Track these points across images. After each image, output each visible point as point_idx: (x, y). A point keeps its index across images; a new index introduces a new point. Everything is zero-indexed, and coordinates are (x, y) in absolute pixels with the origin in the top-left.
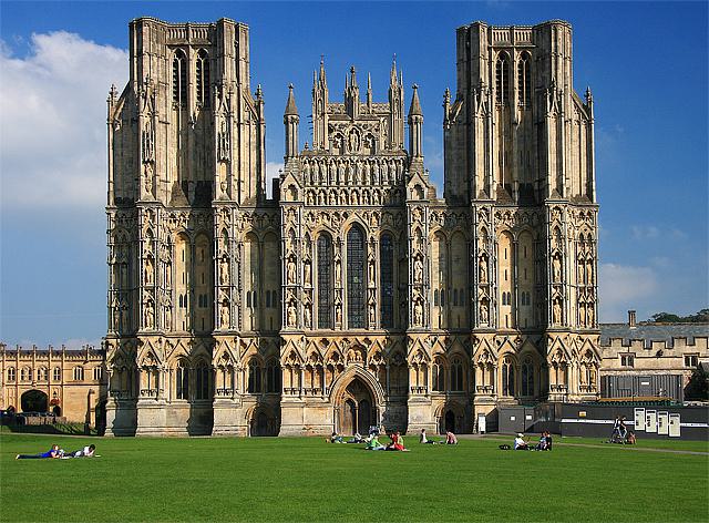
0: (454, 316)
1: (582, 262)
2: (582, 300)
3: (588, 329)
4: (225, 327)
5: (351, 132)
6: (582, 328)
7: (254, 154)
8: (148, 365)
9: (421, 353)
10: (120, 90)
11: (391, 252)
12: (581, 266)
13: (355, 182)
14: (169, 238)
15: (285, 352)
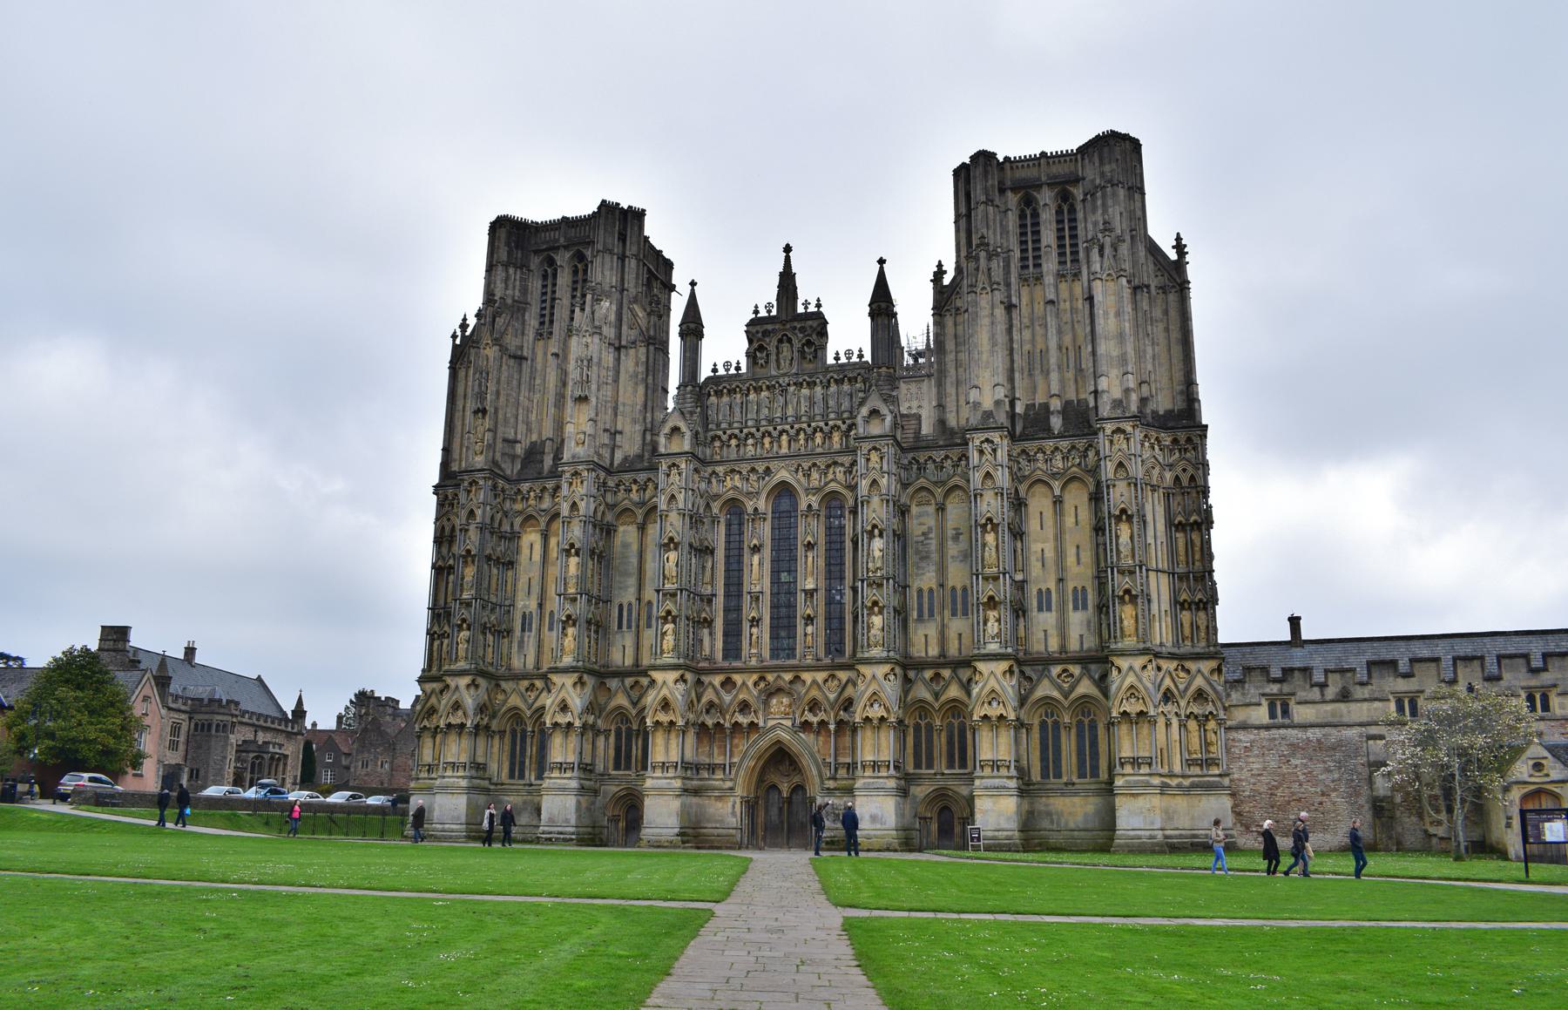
0: (952, 634)
1: (1180, 527)
2: (1184, 596)
3: (1197, 650)
4: (568, 660)
5: (780, 341)
6: (1187, 648)
7: (641, 390)
8: (453, 722)
10: (472, 322)
11: (842, 527)
12: (1180, 535)
15: (651, 699)
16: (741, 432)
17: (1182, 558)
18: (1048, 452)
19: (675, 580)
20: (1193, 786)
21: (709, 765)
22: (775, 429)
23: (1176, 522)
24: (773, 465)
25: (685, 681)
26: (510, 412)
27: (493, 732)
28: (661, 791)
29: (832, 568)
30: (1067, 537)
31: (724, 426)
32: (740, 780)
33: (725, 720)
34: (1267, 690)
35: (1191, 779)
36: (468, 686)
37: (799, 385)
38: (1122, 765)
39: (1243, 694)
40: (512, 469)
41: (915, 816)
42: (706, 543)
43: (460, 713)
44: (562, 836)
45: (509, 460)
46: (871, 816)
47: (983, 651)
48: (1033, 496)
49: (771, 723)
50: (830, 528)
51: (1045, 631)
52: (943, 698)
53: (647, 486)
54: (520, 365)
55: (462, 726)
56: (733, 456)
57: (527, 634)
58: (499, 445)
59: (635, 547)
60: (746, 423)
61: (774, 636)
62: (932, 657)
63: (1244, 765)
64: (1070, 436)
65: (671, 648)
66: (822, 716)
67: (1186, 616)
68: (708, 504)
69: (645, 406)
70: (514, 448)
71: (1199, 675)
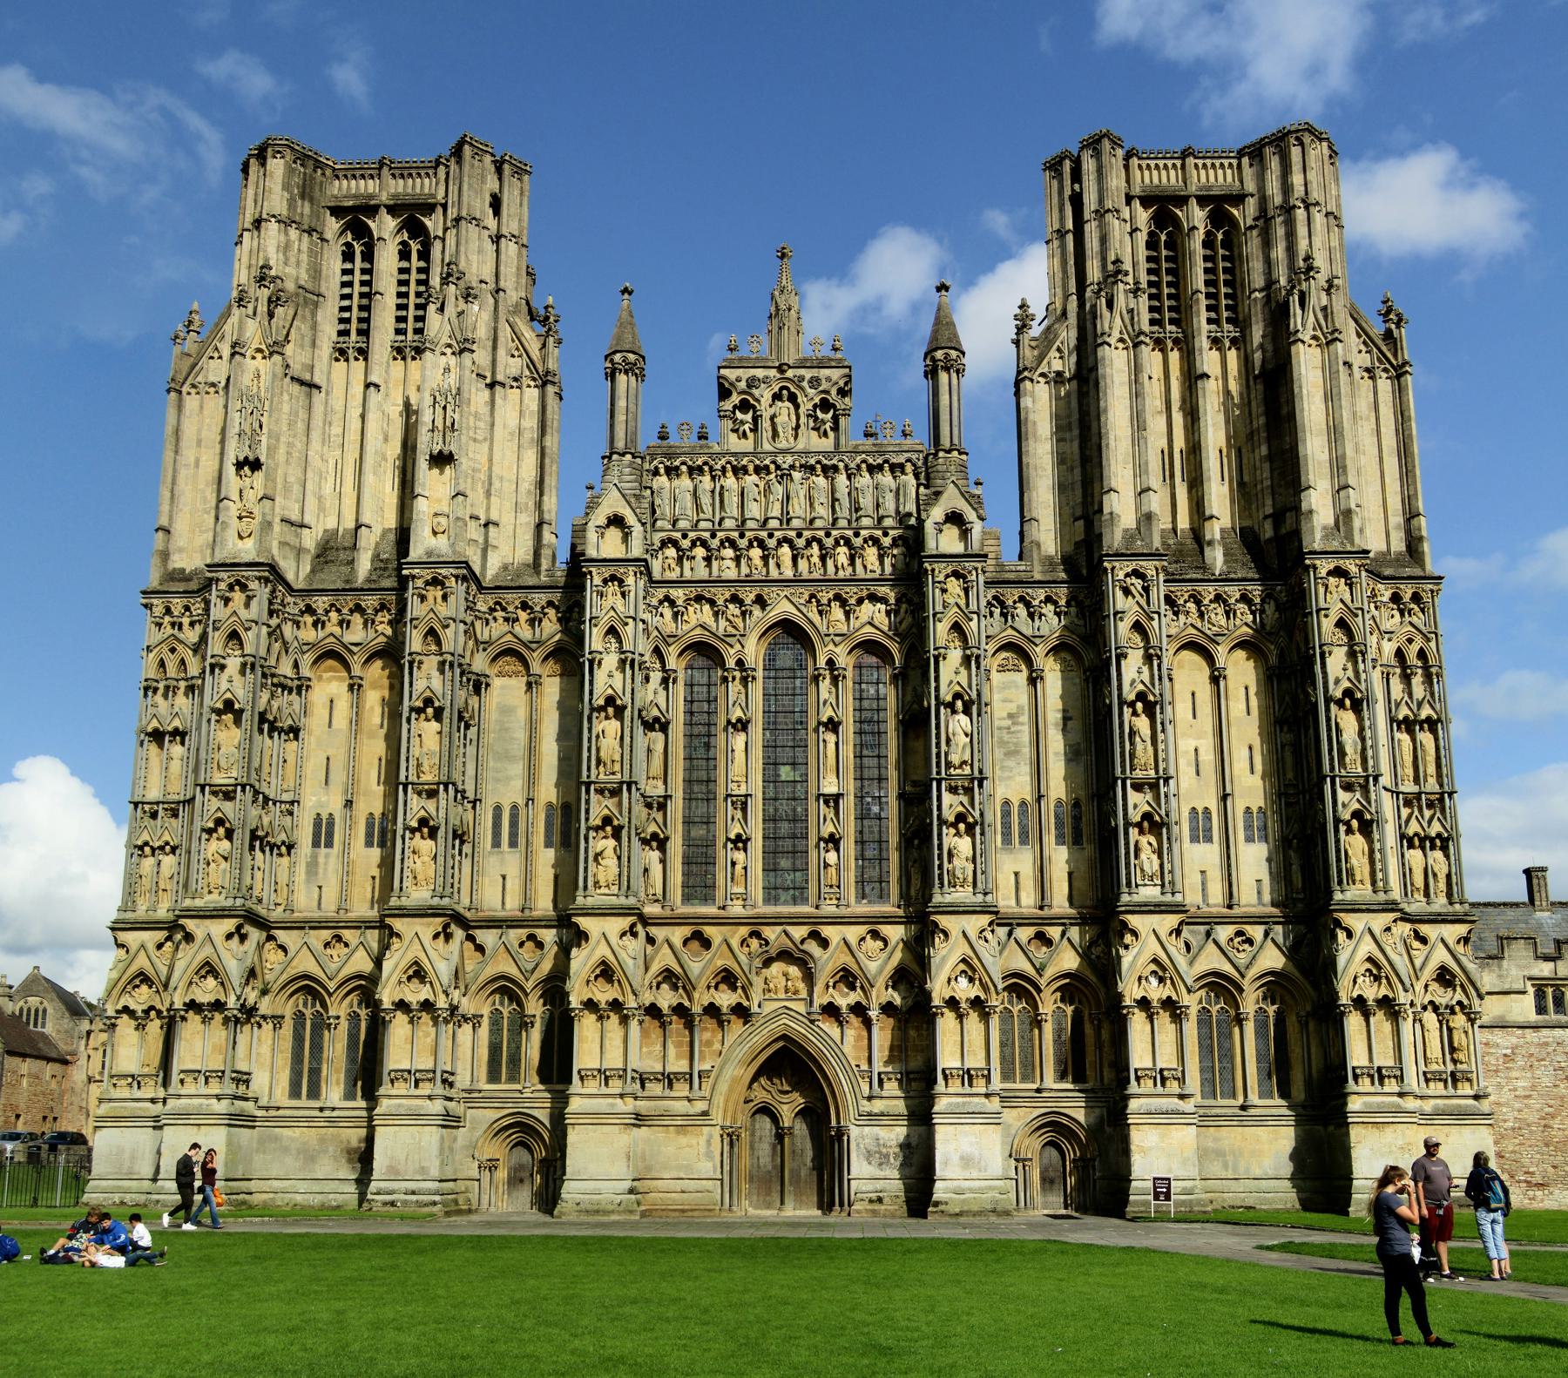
1: (1409, 725)
2: (1413, 828)
5: (777, 397)
6: (1417, 905)
7: (531, 457)
9: (969, 968)
12: (1404, 738)
13: (786, 519)
14: (296, 665)
15: (582, 961)
16: (713, 536)
17: (1410, 771)
18: (1206, 602)
19: (617, 767)
20: (1438, 1113)
21: (663, 1074)
22: (771, 536)
23: (1401, 717)
24: (770, 593)
25: (635, 935)
26: (294, 474)
27: (264, 1017)
28: (597, 1119)
29: (865, 760)
30: (1233, 731)
31: (682, 524)
32: (719, 1100)
33: (690, 999)
34: (1535, 972)
35: (1432, 1102)
36: (229, 937)
37: (812, 469)
38: (1356, 1077)
39: (1500, 976)
40: (297, 572)
41: (1010, 1156)
42: (655, 712)
43: (211, 982)
44: (414, 1198)
45: (292, 556)
46: (962, 1158)
47: (1136, 898)
48: (1181, 666)
49: (769, 1007)
50: (861, 699)
51: (1203, 872)
52: (1050, 972)
53: (545, 614)
54: (310, 396)
55: (218, 1006)
56: (702, 573)
57: (323, 850)
58: (277, 527)
59: (522, 713)
60: (720, 524)
61: (770, 868)
62: (1029, 907)
63: (1504, 1082)
64: (1238, 580)
65: (611, 879)
66: (854, 997)
67: (1415, 857)
68: (657, 647)
69: (541, 483)
70: (298, 536)
71: (1441, 945)
